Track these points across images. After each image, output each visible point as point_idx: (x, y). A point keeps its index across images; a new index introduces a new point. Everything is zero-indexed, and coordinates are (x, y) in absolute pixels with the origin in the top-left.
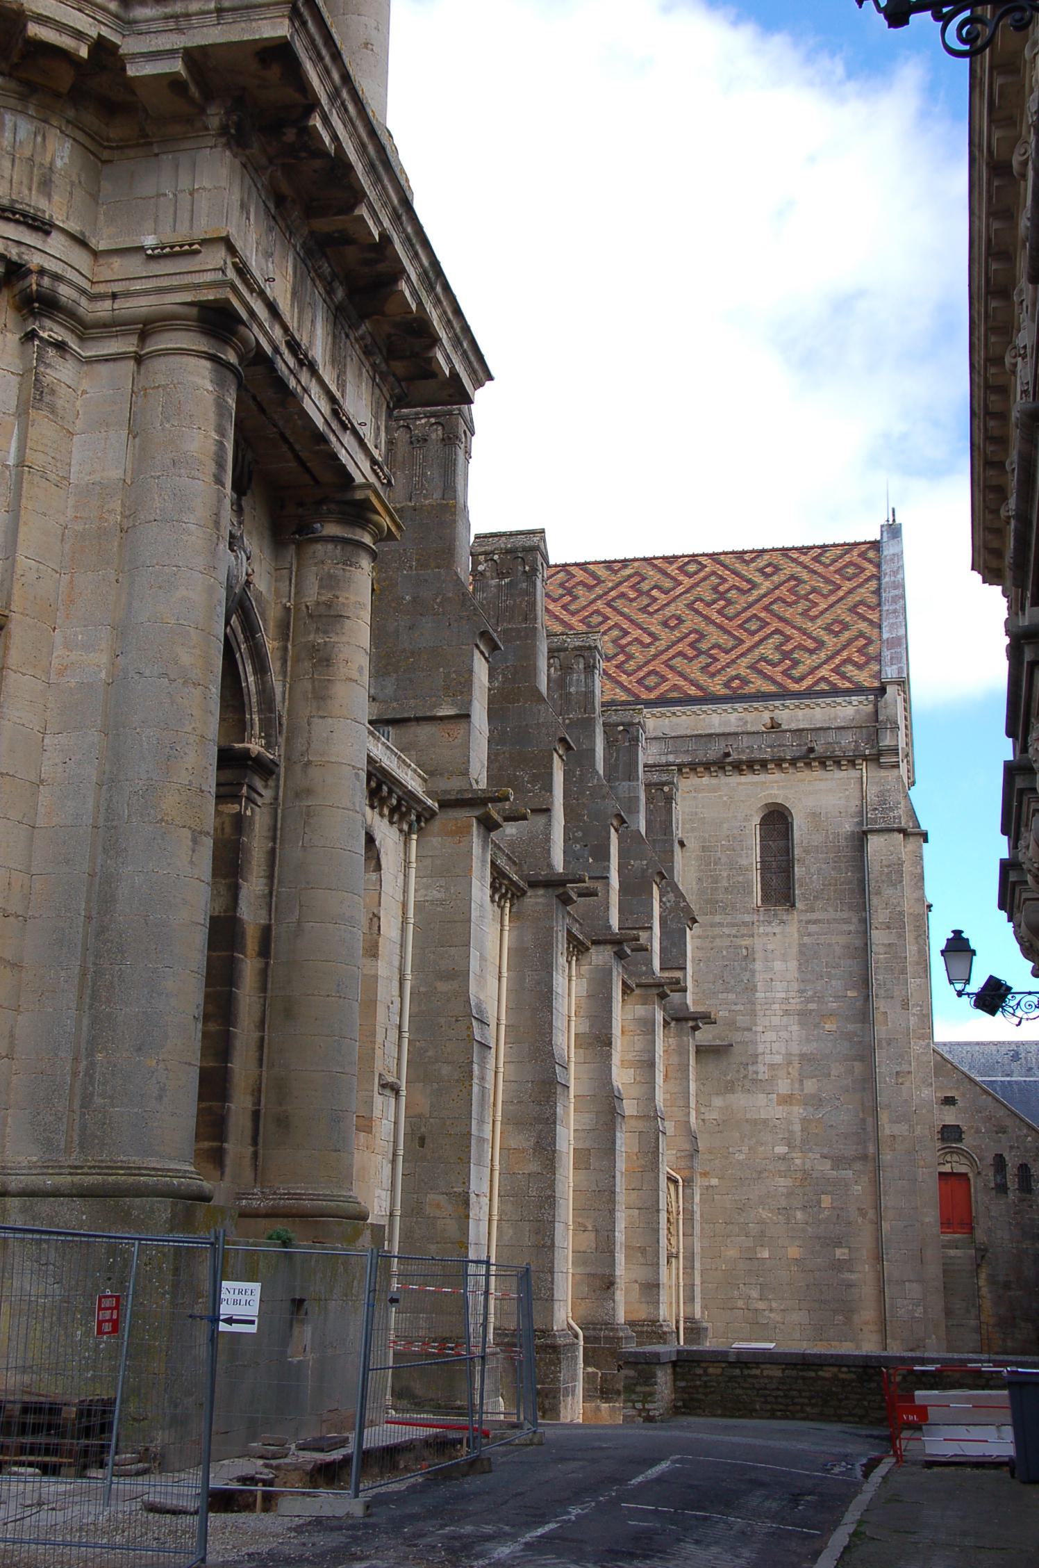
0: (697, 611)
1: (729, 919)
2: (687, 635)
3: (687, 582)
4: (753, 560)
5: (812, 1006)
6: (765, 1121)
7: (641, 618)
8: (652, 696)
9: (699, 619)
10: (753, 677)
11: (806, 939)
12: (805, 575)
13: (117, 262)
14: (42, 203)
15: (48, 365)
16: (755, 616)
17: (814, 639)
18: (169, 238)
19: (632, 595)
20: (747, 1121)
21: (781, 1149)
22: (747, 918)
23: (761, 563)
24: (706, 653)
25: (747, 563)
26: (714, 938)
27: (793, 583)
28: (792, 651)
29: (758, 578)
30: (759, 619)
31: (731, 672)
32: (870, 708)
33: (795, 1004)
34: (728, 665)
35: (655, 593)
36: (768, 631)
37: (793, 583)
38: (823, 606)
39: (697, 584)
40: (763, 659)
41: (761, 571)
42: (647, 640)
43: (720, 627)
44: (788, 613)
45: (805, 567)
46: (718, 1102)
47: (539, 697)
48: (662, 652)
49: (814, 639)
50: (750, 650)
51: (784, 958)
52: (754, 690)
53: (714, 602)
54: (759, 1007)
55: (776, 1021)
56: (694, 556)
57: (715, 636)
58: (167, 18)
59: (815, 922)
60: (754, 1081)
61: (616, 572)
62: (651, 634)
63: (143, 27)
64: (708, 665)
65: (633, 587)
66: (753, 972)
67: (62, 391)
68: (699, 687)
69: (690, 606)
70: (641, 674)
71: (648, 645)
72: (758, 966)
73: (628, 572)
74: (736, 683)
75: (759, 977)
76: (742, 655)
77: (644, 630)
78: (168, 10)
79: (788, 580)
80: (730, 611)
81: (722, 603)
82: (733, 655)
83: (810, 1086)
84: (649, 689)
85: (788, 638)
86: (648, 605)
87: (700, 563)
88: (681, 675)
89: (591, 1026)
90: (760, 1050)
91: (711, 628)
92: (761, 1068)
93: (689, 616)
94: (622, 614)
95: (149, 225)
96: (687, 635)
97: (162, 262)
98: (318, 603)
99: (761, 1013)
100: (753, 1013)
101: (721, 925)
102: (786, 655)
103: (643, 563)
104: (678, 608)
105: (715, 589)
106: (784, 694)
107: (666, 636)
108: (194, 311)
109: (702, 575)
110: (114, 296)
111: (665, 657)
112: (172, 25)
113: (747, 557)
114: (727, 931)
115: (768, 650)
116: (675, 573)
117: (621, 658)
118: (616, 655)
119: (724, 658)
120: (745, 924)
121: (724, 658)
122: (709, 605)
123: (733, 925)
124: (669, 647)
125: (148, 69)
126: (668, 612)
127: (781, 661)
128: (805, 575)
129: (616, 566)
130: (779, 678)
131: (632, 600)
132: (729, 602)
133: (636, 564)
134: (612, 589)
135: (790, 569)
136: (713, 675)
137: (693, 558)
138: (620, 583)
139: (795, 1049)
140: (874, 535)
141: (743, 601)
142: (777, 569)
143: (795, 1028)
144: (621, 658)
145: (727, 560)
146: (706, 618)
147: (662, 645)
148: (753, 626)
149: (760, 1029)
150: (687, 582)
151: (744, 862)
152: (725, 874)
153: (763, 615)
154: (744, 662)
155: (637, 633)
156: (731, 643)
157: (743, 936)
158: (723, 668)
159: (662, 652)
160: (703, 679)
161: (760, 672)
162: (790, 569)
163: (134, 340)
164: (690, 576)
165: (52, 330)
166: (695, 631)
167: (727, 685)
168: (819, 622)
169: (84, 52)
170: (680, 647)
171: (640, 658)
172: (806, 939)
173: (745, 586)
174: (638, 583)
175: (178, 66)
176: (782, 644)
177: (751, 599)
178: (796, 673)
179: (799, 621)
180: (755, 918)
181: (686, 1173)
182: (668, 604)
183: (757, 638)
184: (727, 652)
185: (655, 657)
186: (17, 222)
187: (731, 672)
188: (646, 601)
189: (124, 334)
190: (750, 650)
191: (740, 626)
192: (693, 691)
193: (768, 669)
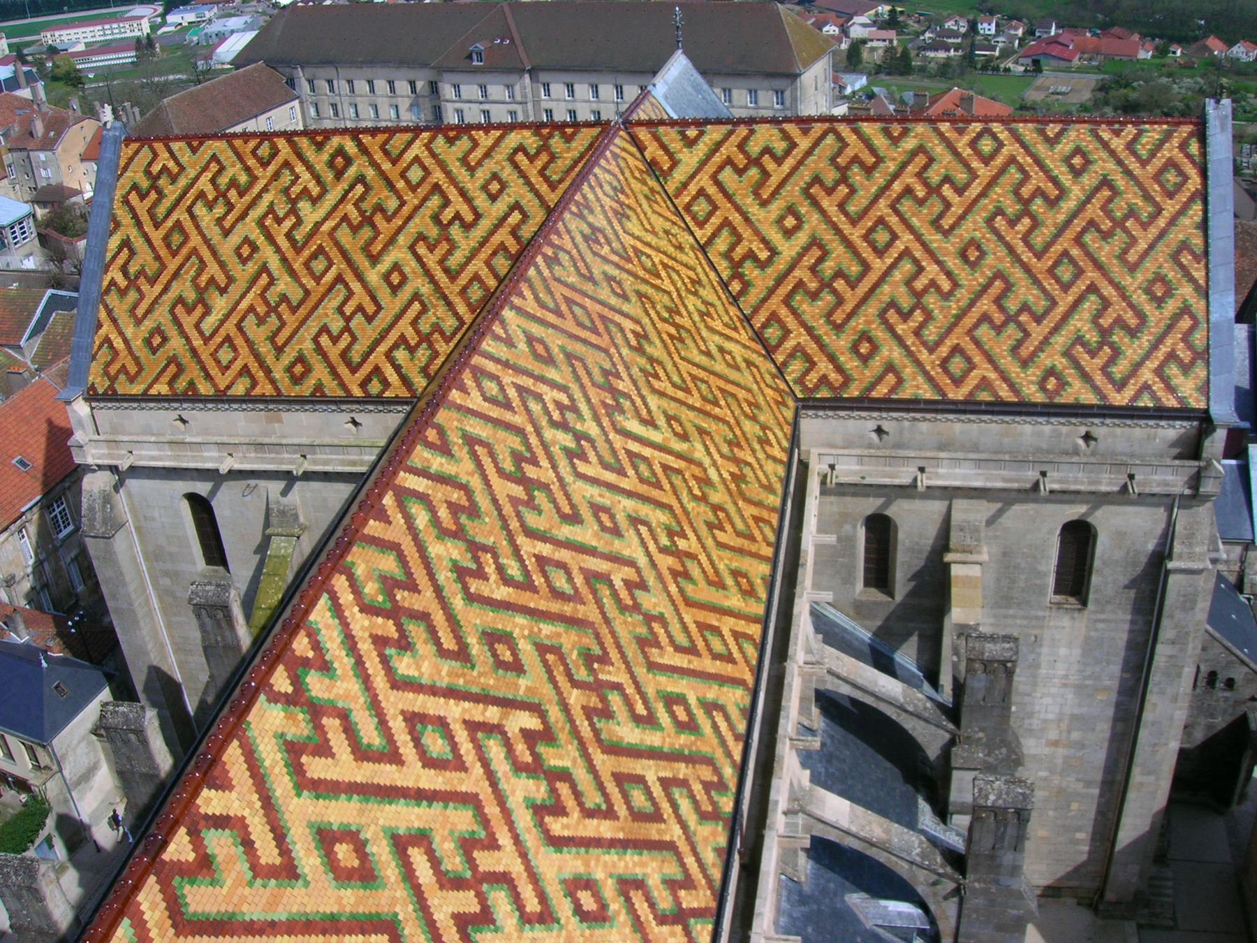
1: (1021, 613)
5: (1088, 682)
11: (1093, 634)
21: (1043, 774)
22: (1040, 614)
33: (1073, 679)
51: (1070, 645)
59: (1103, 621)
66: (1039, 654)
75: (1044, 660)
83: (1076, 735)
90: (1037, 708)
100: (1035, 684)
101: (1014, 617)
120: (1037, 618)
123: (1025, 618)
139: (1068, 710)
143: (1070, 696)
149: (1038, 695)
151: (1042, 568)
152: (1023, 577)
172: (1093, 634)
180: (1047, 614)
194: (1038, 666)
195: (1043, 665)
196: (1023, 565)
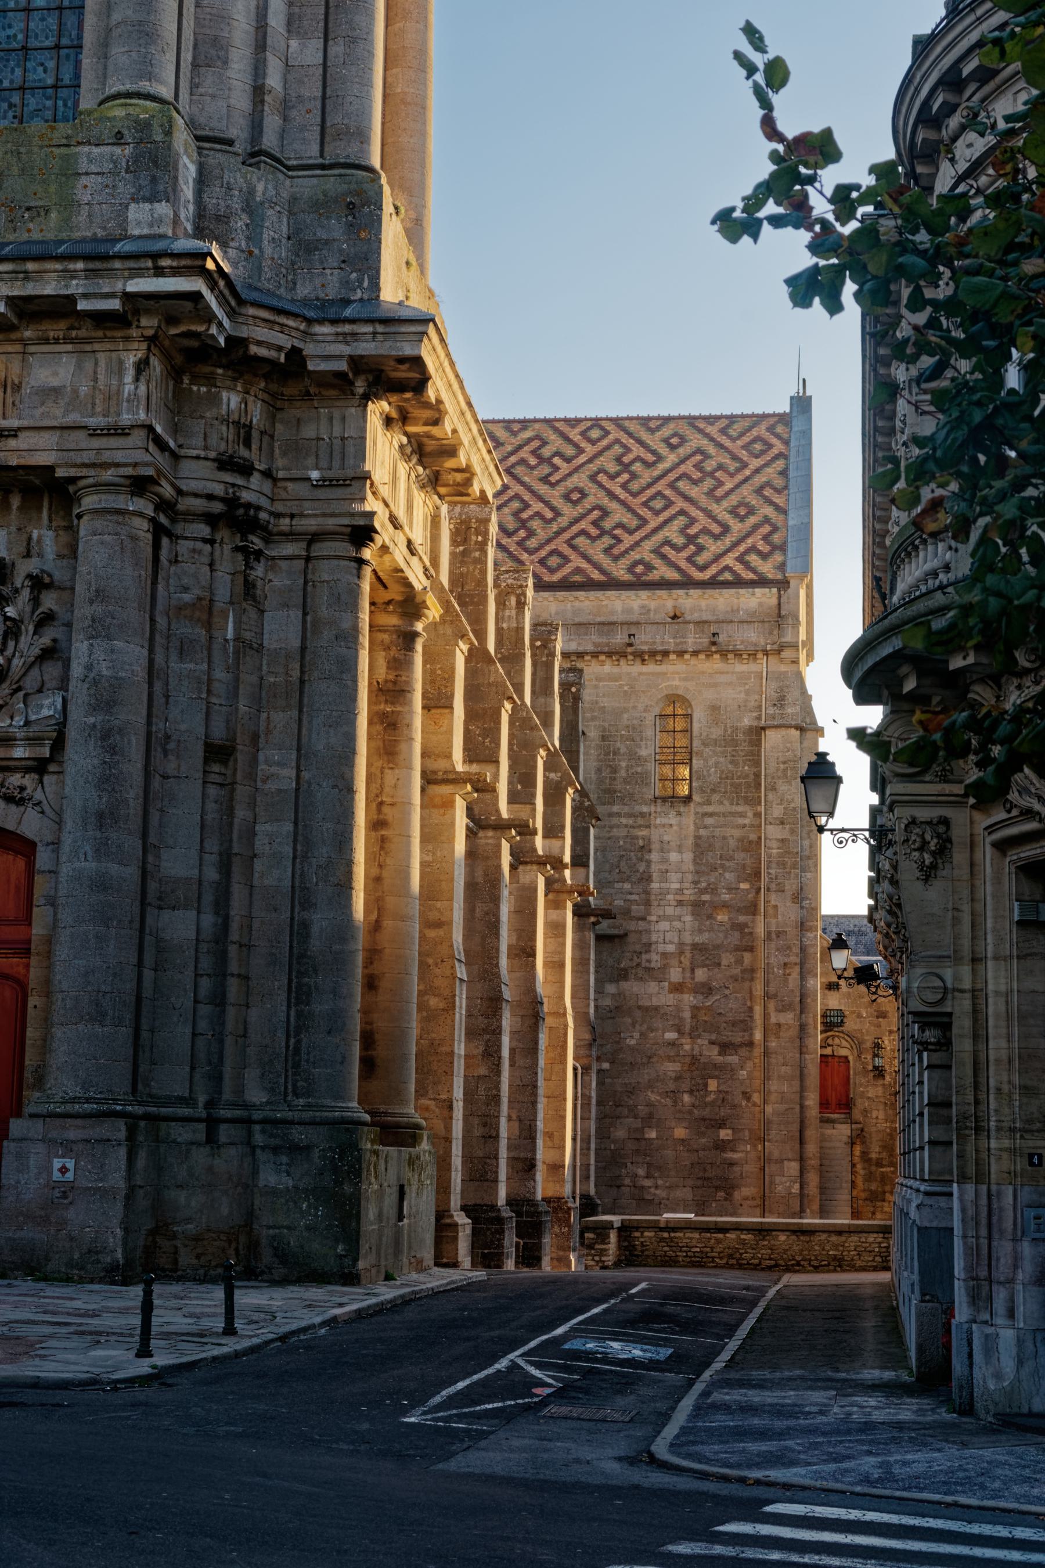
0: (601, 485)
1: (626, 809)
2: (590, 511)
3: (590, 450)
4: (658, 428)
5: (706, 897)
6: (656, 1009)
7: (543, 489)
8: (556, 578)
9: (601, 494)
10: (657, 562)
12: (712, 450)
13: (290, 485)
14: (243, 452)
15: (252, 568)
16: (659, 493)
17: (720, 523)
18: (329, 474)
19: (533, 461)
20: (639, 1007)
21: (671, 1036)
23: (666, 432)
24: (609, 533)
25: (652, 431)
26: (611, 827)
27: (699, 457)
28: (696, 536)
29: (663, 450)
30: (664, 497)
31: (635, 555)
32: (774, 601)
33: (689, 894)
34: (632, 548)
35: (557, 460)
36: (672, 511)
37: (699, 457)
38: (729, 486)
39: (599, 454)
40: (667, 542)
41: (666, 441)
42: (549, 515)
43: (623, 503)
44: (694, 492)
45: (712, 439)
46: (611, 988)
47: (490, 660)
48: (564, 530)
49: (720, 523)
50: (655, 531)
51: (680, 849)
52: (657, 578)
53: (618, 474)
54: (653, 897)
55: (670, 911)
56: (597, 419)
57: (619, 515)
58: (337, 334)
59: (711, 815)
60: (649, 969)
61: (514, 434)
62: (553, 509)
63: (320, 338)
64: (612, 547)
65: (533, 452)
67: (259, 583)
68: (602, 571)
69: (593, 478)
70: (543, 553)
71: (549, 521)
72: (654, 856)
73: (527, 434)
74: (639, 569)
76: (647, 537)
77: (547, 504)
78: (339, 330)
79: (694, 454)
80: (635, 486)
81: (626, 476)
82: (637, 536)
83: (701, 974)
84: (552, 571)
85: (693, 521)
86: (550, 474)
87: (602, 428)
88: (584, 556)
89: (518, 939)
90: (654, 938)
91: (614, 506)
92: (654, 957)
93: (592, 489)
94: (523, 484)
95: (311, 461)
96: (590, 511)
97: (323, 490)
98: (386, 681)
99: (655, 903)
100: (648, 903)
101: (619, 815)
102: (691, 540)
103: (545, 426)
104: (580, 480)
105: (618, 460)
106: (687, 583)
107: (569, 512)
108: (349, 529)
109: (605, 442)
110: (292, 516)
111: (567, 535)
112: (341, 338)
113: (652, 424)
114: (624, 821)
115: (672, 532)
116: (577, 438)
117: (522, 533)
118: (516, 531)
119: (628, 540)
120: (642, 815)
121: (628, 540)
122: (612, 477)
123: (630, 815)
124: (571, 524)
125: (323, 366)
126: (570, 484)
127: (685, 546)
128: (712, 450)
129: (516, 427)
130: (683, 565)
131: (532, 468)
132: (634, 476)
133: (537, 426)
134: (511, 454)
135: (696, 441)
136: (616, 558)
137: (596, 422)
138: (520, 447)
139: (688, 939)
140: (784, 407)
141: (647, 475)
142: (683, 440)
143: (688, 918)
144: (522, 533)
145: (632, 427)
146: (610, 493)
147: (564, 521)
148: (658, 504)
149: (653, 918)
150: (590, 450)
151: (643, 753)
152: (624, 764)
153: (668, 492)
154: (649, 545)
155: (537, 506)
156: (635, 523)
157: (640, 826)
158: (627, 551)
159: (564, 530)
160: (605, 561)
161: (664, 557)
162: (696, 441)
163: (304, 545)
164: (593, 442)
165: (256, 542)
166: (598, 507)
167: (630, 569)
168: (725, 504)
169: (282, 359)
170: (584, 524)
171: (542, 535)
172: (702, 832)
173: (650, 458)
174: (539, 448)
175: (343, 366)
176: (687, 527)
177: (656, 473)
178: (700, 560)
179: (704, 501)
180: (653, 808)
181: (585, 1061)
182: (570, 474)
183: (661, 518)
184: (631, 532)
185: (558, 534)
186: (233, 471)
187: (635, 555)
188: (546, 469)
189: (296, 540)
190: (655, 531)
191: (645, 504)
192: (596, 575)
193: (671, 554)
194: (649, 879)
195: (655, 876)
196: (623, 750)
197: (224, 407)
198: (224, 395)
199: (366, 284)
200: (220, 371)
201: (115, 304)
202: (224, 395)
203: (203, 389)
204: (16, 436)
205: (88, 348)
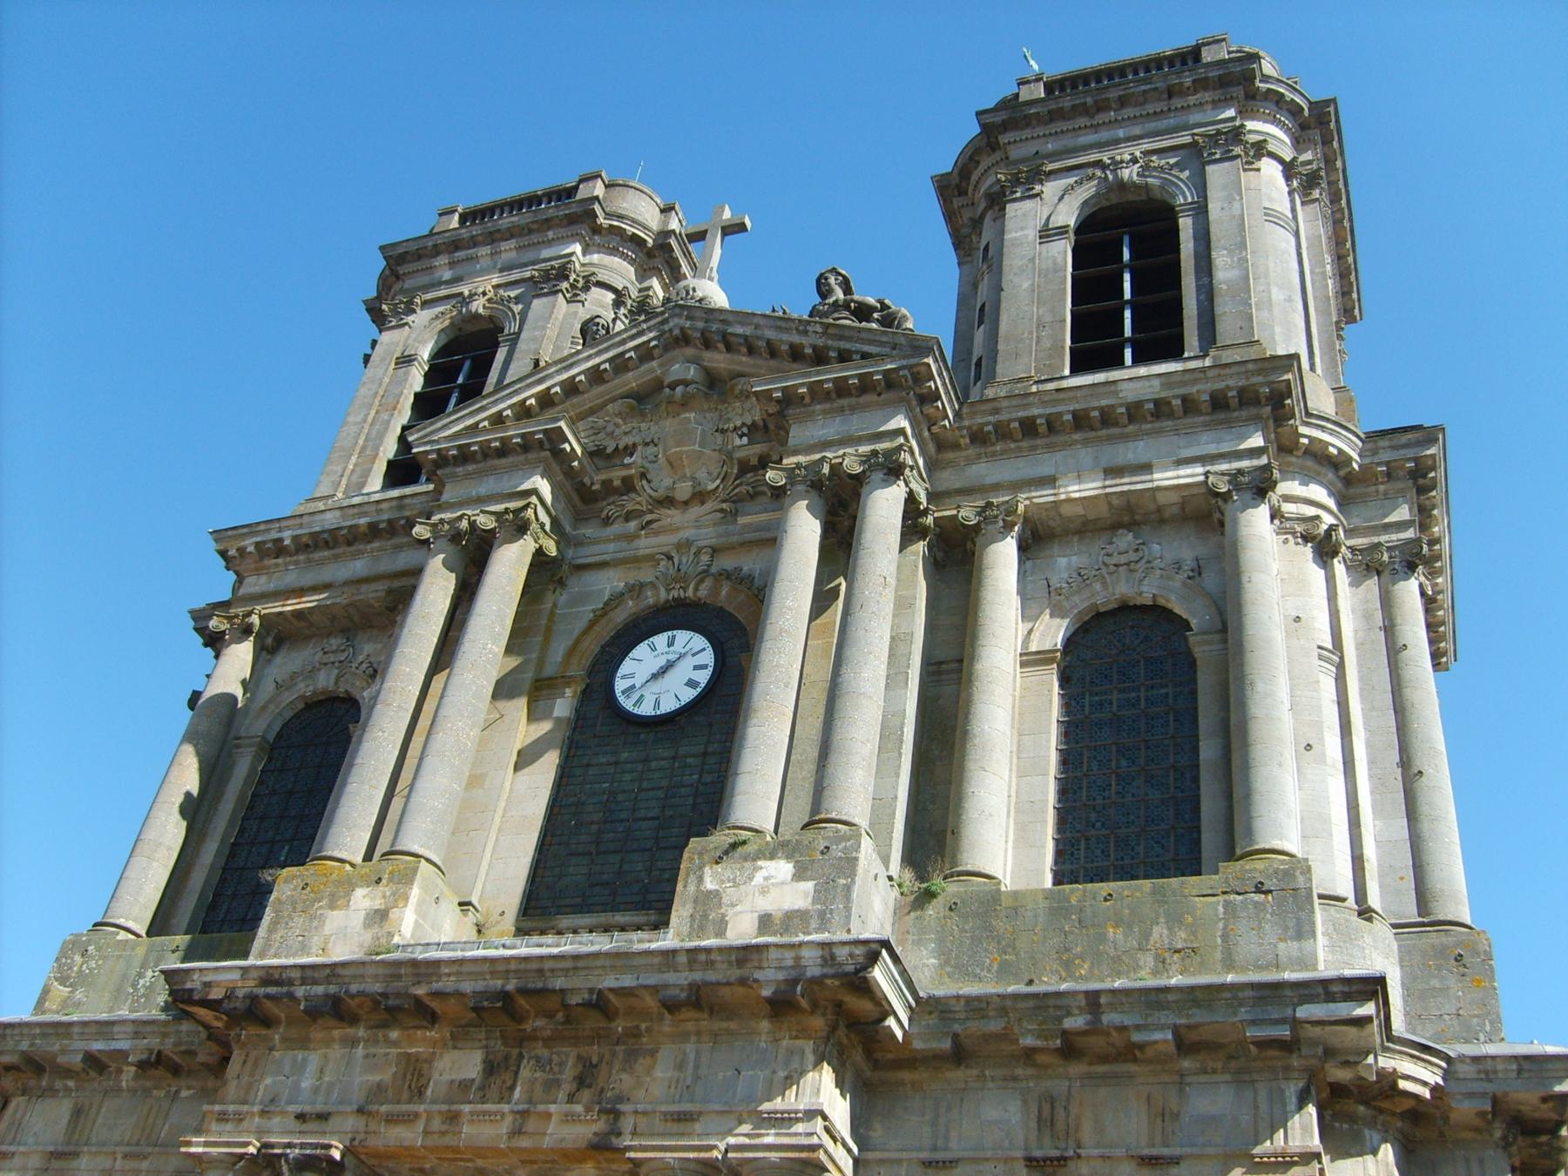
197: (1368, 1144)
198: (1366, 1132)
199: (1488, 1028)
200: (1361, 1108)
201: (1284, 1032)
202: (1366, 1132)
203: (1345, 1126)
204: (1177, 1163)
205: (1247, 1078)
